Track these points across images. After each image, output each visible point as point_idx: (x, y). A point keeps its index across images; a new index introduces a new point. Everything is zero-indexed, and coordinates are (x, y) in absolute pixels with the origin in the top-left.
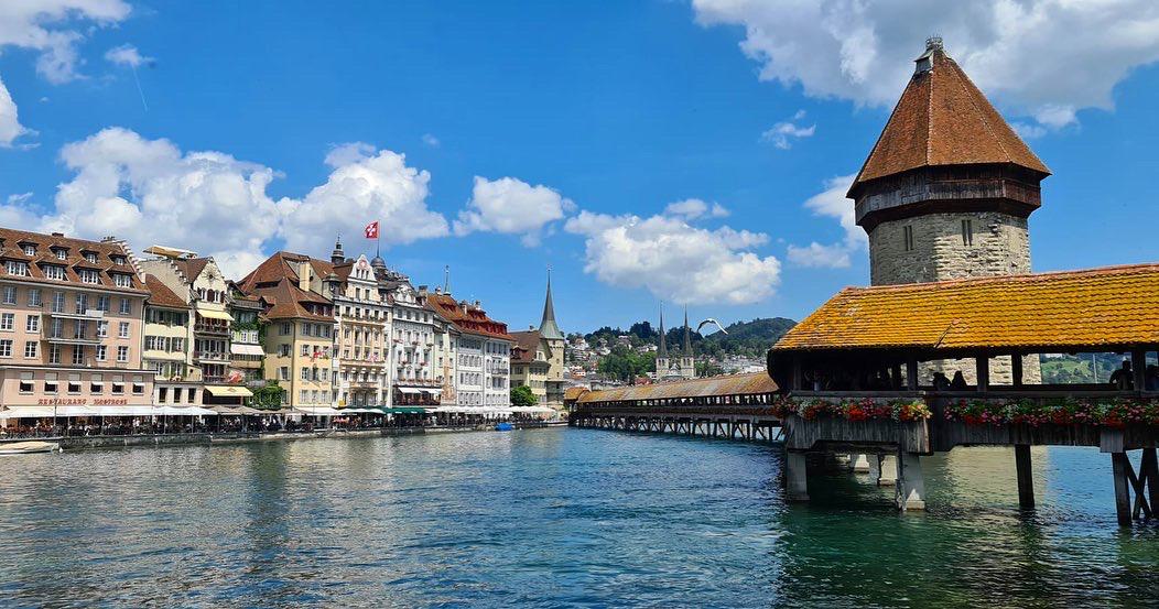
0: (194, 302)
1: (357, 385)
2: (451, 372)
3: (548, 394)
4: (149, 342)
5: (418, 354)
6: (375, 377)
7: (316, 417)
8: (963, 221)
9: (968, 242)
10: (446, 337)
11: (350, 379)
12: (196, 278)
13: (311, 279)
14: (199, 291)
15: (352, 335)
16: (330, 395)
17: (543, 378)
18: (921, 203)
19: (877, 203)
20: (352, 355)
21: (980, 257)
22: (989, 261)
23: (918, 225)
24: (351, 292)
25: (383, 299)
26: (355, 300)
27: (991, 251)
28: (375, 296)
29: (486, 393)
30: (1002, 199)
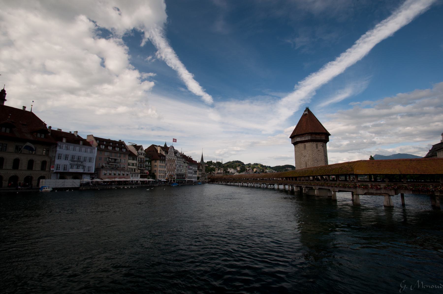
1: (169, 174)
2: (187, 172)
3: (202, 176)
5: (181, 168)
6: (173, 172)
10: (186, 164)
11: (169, 173)
13: (161, 151)
15: (169, 163)
16: (164, 176)
17: (201, 173)
18: (308, 140)
19: (298, 139)
21: (320, 151)
22: (321, 152)
23: (308, 144)
24: (169, 154)
25: (175, 155)
26: (170, 155)
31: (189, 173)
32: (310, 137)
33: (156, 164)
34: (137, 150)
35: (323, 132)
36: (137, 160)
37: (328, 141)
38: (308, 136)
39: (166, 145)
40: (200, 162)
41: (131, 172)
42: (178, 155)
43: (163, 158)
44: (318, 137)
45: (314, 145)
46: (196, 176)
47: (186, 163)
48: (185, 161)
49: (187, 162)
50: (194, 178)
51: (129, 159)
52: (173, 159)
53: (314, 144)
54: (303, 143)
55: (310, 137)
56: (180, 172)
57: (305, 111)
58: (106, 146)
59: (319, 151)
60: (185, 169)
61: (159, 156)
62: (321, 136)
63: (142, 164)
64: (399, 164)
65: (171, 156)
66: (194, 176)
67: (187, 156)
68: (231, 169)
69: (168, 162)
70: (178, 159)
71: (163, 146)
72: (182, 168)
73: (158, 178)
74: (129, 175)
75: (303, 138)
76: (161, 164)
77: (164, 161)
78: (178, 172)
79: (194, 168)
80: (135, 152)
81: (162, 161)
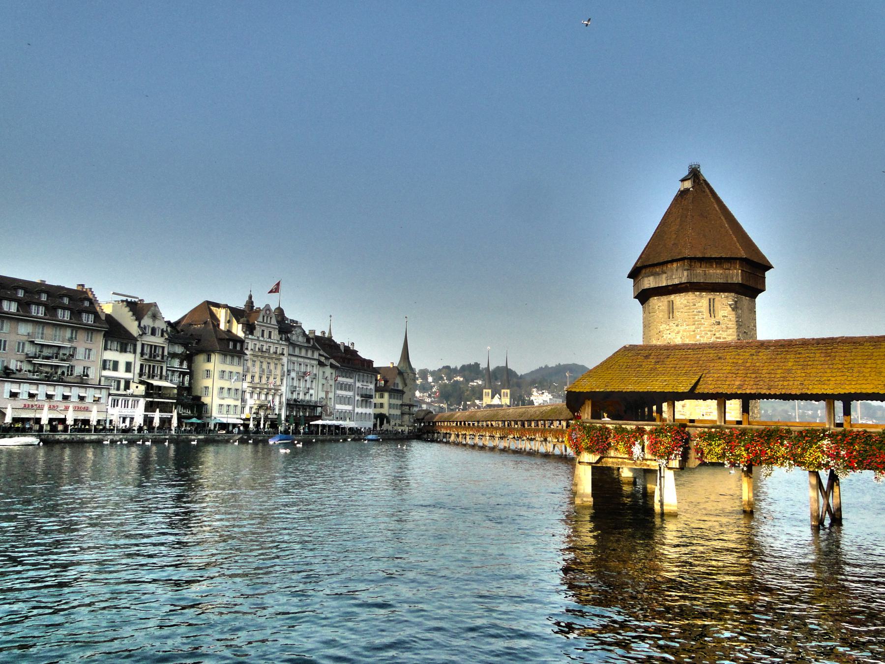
1: (258, 402)
2: (331, 395)
3: (403, 414)
5: (306, 381)
8: (710, 300)
9: (713, 315)
10: (328, 371)
11: (255, 396)
13: (229, 322)
14: (145, 328)
15: (258, 364)
16: (239, 409)
17: (399, 402)
18: (681, 284)
20: (257, 380)
23: (679, 300)
25: (281, 339)
28: (275, 335)
29: (356, 411)
32: (685, 273)
33: (208, 369)
34: (136, 320)
36: (135, 352)
37: (763, 290)
38: (680, 271)
39: (250, 303)
40: (396, 365)
41: (112, 392)
42: (298, 337)
43: (235, 346)
44: (716, 274)
45: (700, 304)
46: (370, 411)
47: (329, 367)
48: (323, 359)
49: (332, 361)
50: (362, 416)
51: (106, 349)
52: (272, 350)
53: (703, 301)
55: (685, 273)
56: (301, 397)
57: (683, 180)
58: (51, 309)
59: (719, 323)
61: (221, 340)
62: (729, 269)
63: (154, 366)
64: (719, 358)
65: (266, 342)
66: (359, 410)
67: (338, 342)
68: (543, 393)
69: (254, 361)
70: (297, 350)
71: (241, 304)
72: (312, 381)
73: (215, 413)
74: (102, 401)
75: (664, 276)
76: (228, 368)
77: (240, 358)
78: (295, 396)
79: (358, 384)
80: (132, 327)
81: (233, 356)
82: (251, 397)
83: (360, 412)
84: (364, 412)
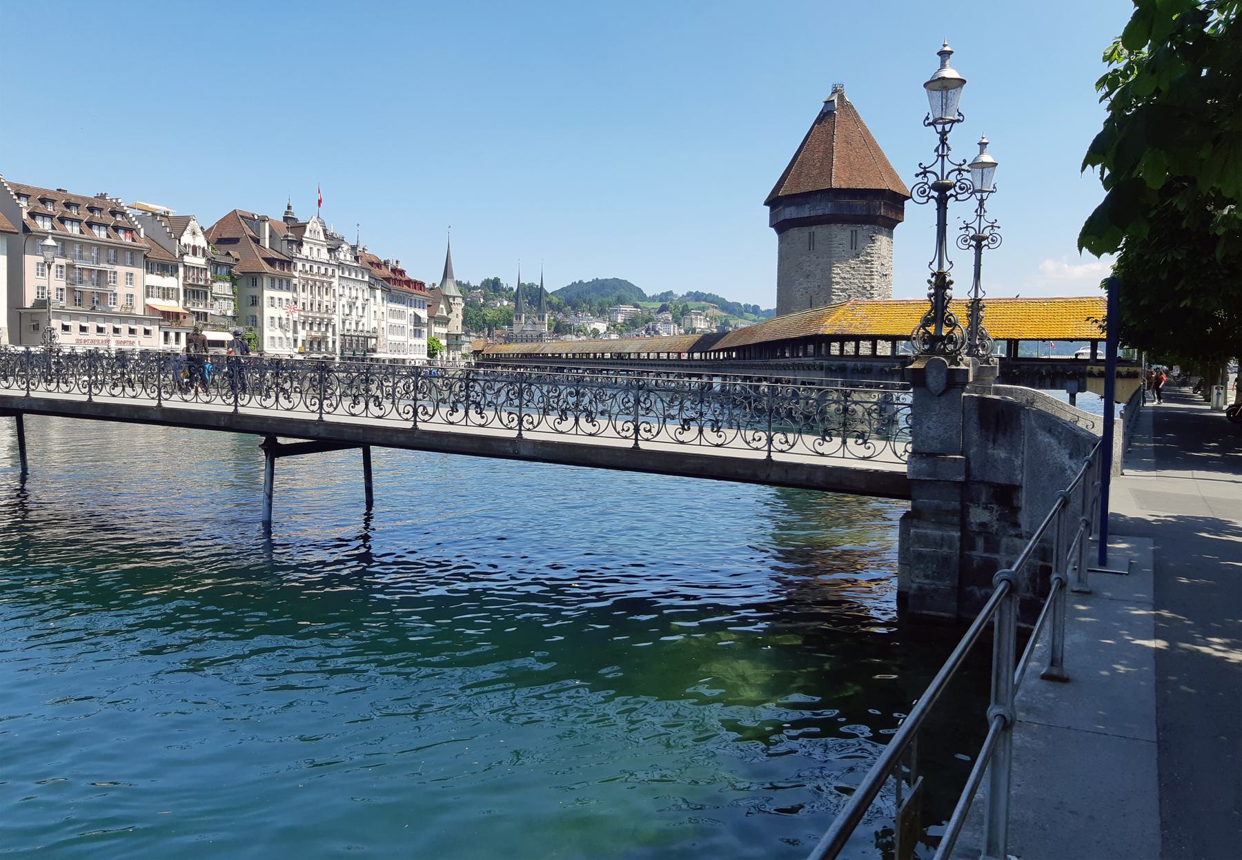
0: (182, 255)
4: (148, 291)
5: (357, 308)
7: (281, 360)
8: (852, 231)
10: (378, 293)
11: (308, 328)
12: (182, 235)
14: (185, 246)
17: (444, 330)
19: (790, 213)
23: (819, 231)
24: (305, 250)
25: (331, 257)
26: (309, 258)
27: (869, 253)
28: (325, 255)
30: (880, 216)
31: (393, 328)
32: (830, 205)
35: (878, 187)
42: (345, 256)
54: (806, 228)
55: (830, 205)
60: (375, 315)
65: (315, 262)
75: (808, 206)
76: (277, 294)
82: (303, 328)
83: (413, 344)
84: (417, 344)
